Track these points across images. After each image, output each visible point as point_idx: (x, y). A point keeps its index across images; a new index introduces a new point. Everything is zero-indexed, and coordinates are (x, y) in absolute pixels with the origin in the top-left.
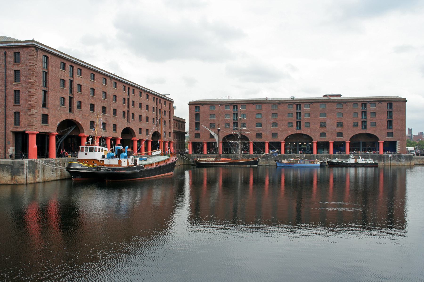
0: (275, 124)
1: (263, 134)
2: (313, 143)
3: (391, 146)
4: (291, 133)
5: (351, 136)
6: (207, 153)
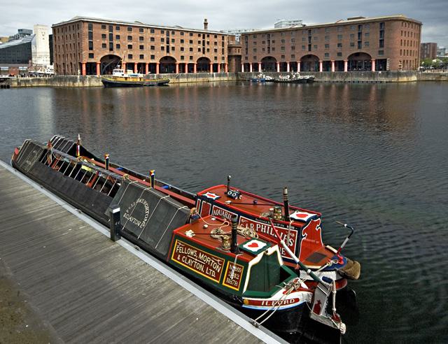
3: (382, 64)
5: (349, 55)
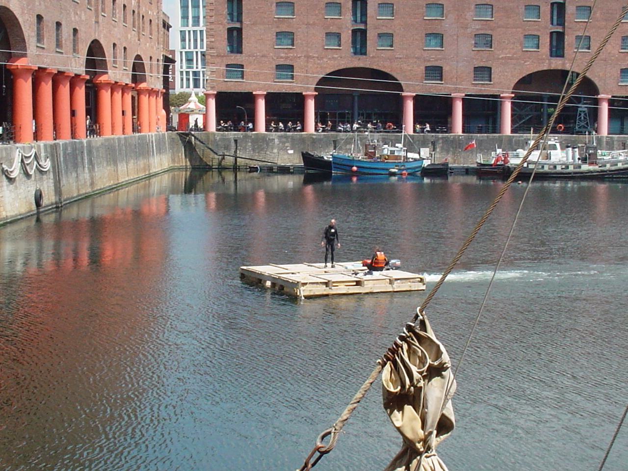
0: (485, 40)
1: (446, 69)
2: (597, 102)
4: (532, 67)
6: (267, 130)
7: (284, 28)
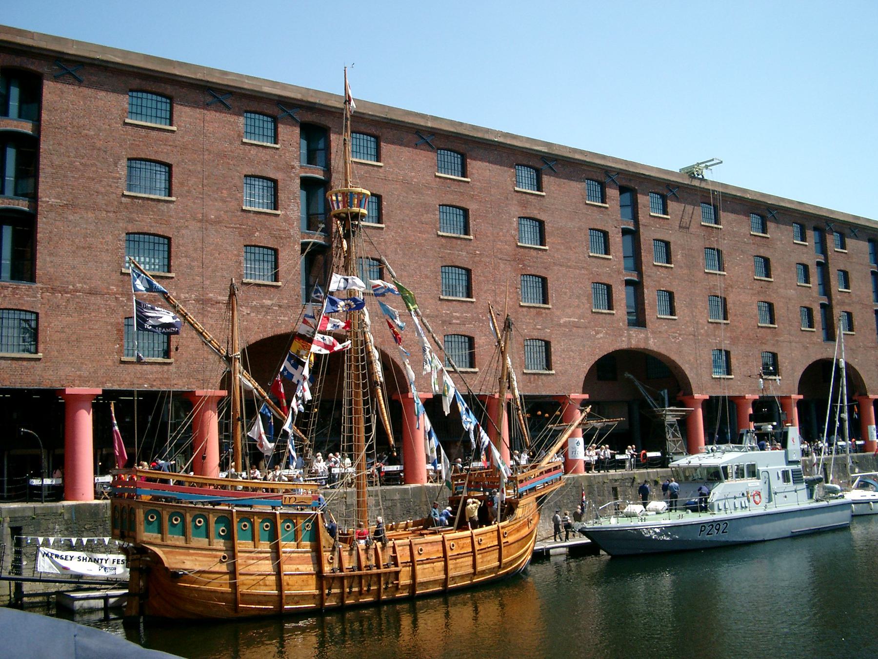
7: (146, 222)
